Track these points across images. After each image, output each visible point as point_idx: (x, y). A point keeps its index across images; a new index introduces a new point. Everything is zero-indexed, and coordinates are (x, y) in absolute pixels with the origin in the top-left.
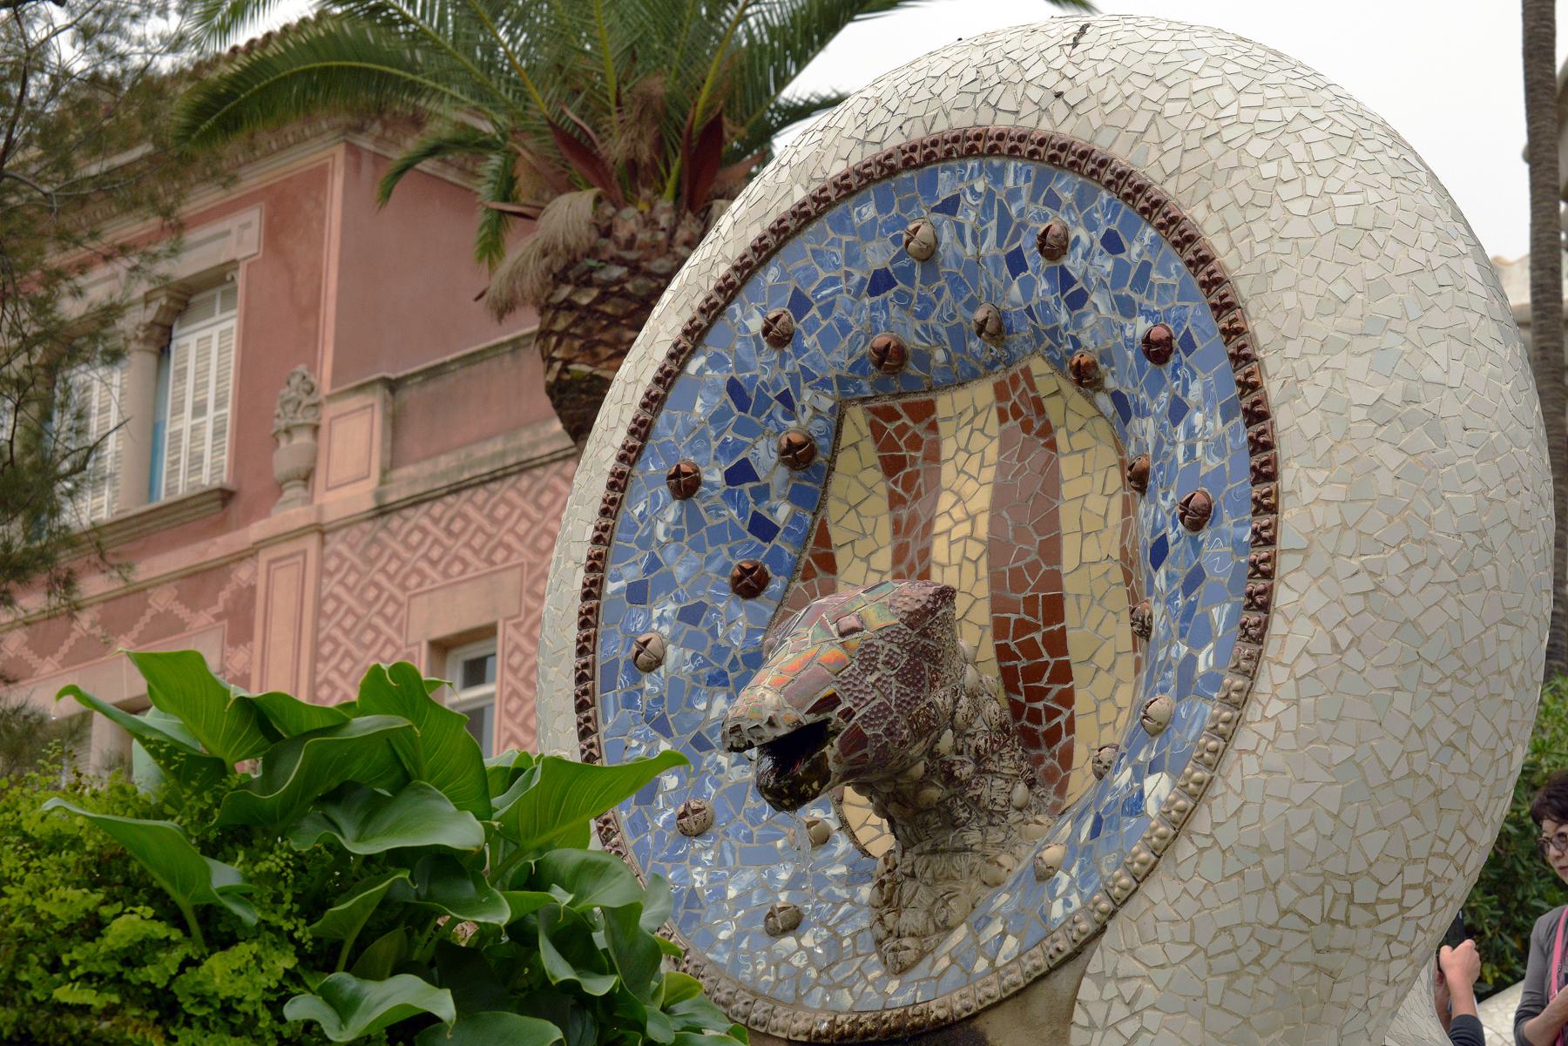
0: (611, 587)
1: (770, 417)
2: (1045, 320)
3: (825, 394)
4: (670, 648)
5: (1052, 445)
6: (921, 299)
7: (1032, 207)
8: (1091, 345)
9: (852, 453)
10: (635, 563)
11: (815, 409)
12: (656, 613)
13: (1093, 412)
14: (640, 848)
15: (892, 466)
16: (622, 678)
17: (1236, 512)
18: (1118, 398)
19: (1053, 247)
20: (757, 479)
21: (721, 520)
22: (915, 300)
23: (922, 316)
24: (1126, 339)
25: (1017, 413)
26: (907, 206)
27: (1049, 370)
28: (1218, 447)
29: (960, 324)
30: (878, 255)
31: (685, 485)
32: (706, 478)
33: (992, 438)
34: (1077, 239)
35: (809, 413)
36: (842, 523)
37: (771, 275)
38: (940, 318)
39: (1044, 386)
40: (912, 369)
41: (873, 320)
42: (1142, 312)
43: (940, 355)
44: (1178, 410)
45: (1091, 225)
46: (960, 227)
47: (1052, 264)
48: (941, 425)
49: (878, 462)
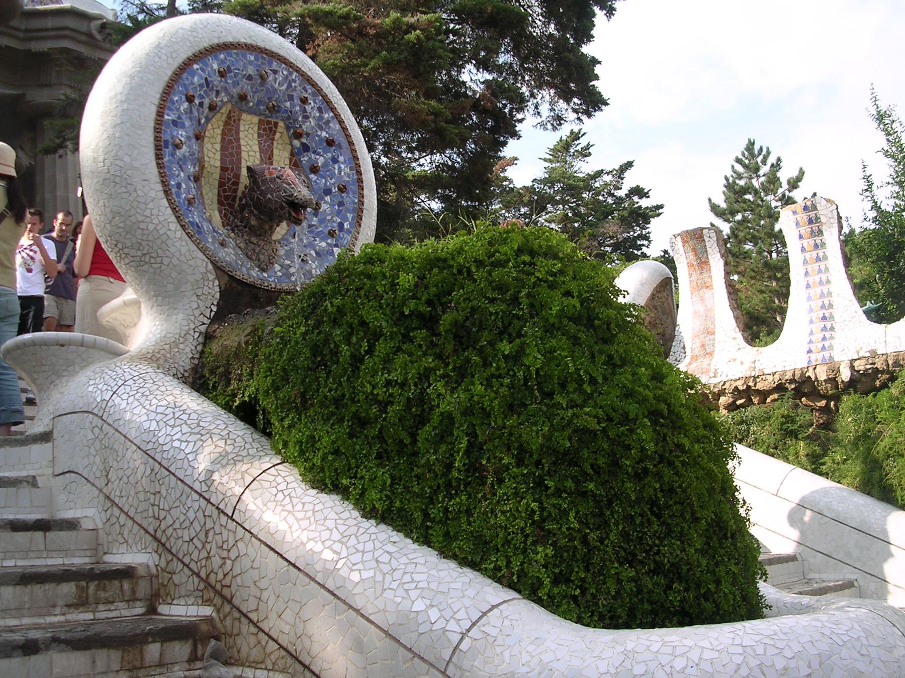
0: (166, 117)
5: (272, 143)
14: (179, 202)
15: (226, 123)
16: (170, 147)
17: (353, 193)
19: (304, 101)
25: (264, 130)
26: (263, 64)
28: (349, 176)
30: (251, 70)
31: (190, 99)
37: (222, 56)
39: (280, 129)
40: (244, 103)
43: (251, 104)
44: (335, 161)
45: (315, 103)
46: (276, 79)
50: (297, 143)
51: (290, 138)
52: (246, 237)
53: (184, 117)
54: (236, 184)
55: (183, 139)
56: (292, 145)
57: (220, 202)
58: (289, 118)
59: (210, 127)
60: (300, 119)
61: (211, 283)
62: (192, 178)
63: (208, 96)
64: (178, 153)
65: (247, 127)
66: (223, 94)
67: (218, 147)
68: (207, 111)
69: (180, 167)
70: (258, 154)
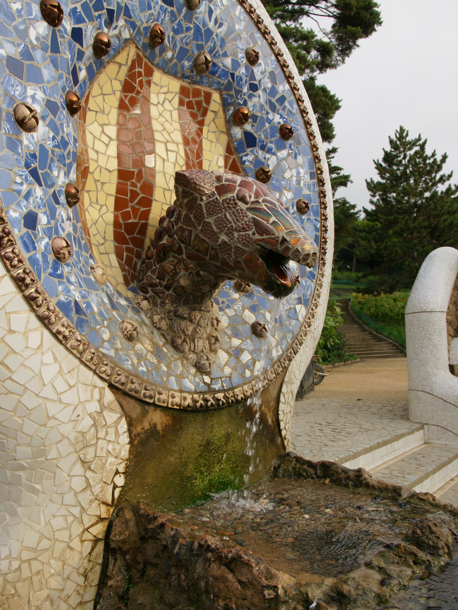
1: (100, 16)
2: (238, 84)
3: (129, 31)
4: (41, 122)
6: (179, 24)
7: (244, 33)
8: (251, 109)
9: (116, 67)
10: (13, 43)
11: (120, 33)
12: (30, 92)
13: (225, 130)
14: (33, 260)
15: (127, 87)
18: (247, 135)
19: (252, 58)
20: (81, 45)
21: (66, 57)
22: (177, 22)
23: (176, 32)
24: (268, 118)
25: (190, 105)
27: (220, 102)
29: (188, 51)
32: (63, 22)
33: (175, 109)
34: (260, 65)
35: (116, 32)
36: (95, 99)
38: (182, 39)
41: (159, 12)
42: (278, 114)
43: (169, 54)
46: (211, 12)
47: (248, 64)
48: (152, 85)
49: (123, 79)
50: (238, 132)
51: (227, 122)
52: (168, 306)
53: (38, 55)
54: (147, 202)
55: (37, 108)
56: (229, 134)
57: (118, 238)
58: (229, 87)
59: (95, 90)
60: (245, 90)
61: (112, 431)
62: (62, 199)
63: (91, 19)
64: (25, 137)
65: (162, 97)
66: (121, 22)
67: (112, 131)
68: (89, 52)
69: (34, 173)
70: (181, 147)
